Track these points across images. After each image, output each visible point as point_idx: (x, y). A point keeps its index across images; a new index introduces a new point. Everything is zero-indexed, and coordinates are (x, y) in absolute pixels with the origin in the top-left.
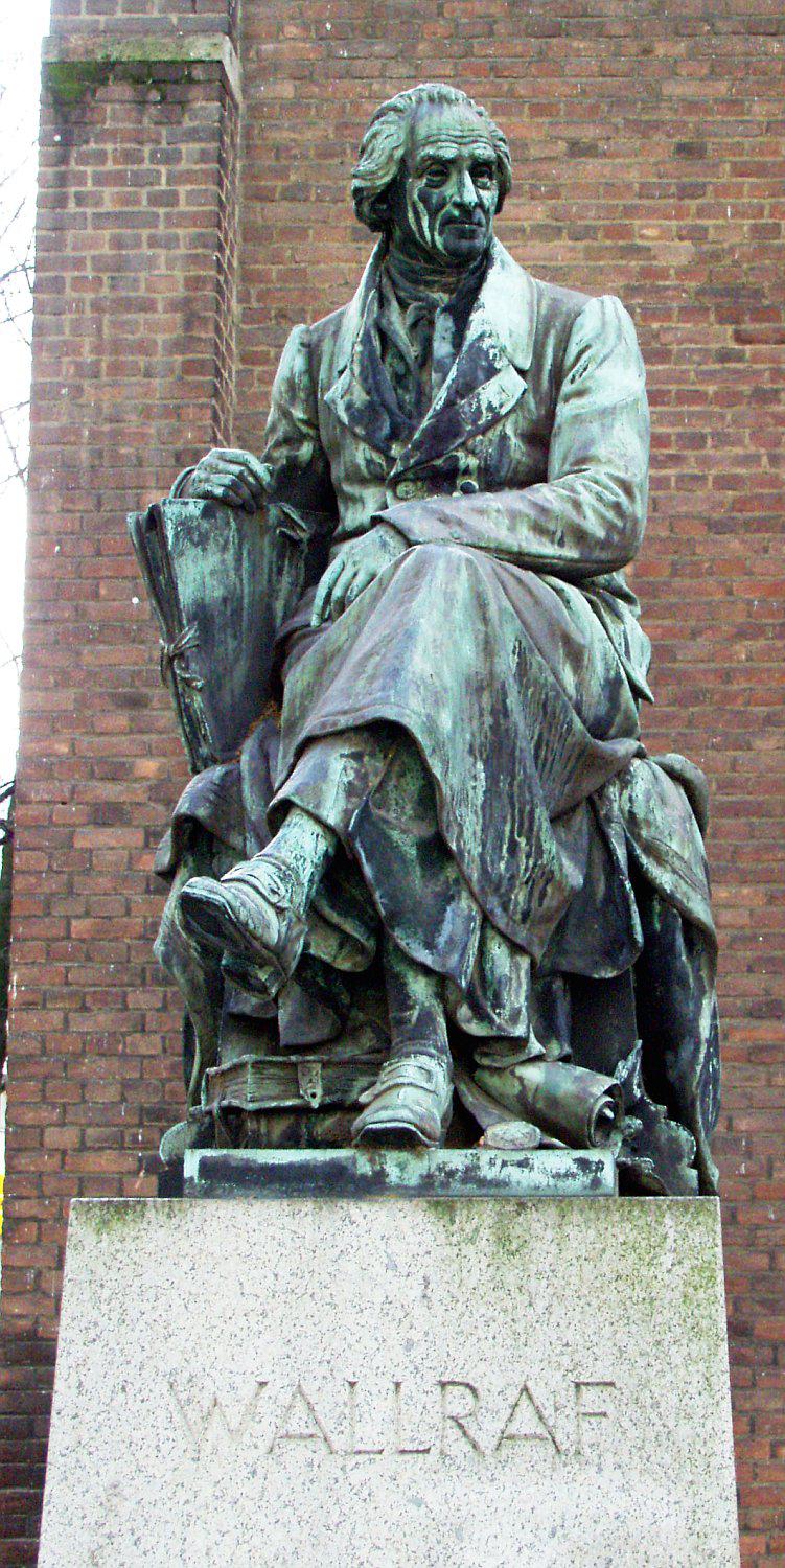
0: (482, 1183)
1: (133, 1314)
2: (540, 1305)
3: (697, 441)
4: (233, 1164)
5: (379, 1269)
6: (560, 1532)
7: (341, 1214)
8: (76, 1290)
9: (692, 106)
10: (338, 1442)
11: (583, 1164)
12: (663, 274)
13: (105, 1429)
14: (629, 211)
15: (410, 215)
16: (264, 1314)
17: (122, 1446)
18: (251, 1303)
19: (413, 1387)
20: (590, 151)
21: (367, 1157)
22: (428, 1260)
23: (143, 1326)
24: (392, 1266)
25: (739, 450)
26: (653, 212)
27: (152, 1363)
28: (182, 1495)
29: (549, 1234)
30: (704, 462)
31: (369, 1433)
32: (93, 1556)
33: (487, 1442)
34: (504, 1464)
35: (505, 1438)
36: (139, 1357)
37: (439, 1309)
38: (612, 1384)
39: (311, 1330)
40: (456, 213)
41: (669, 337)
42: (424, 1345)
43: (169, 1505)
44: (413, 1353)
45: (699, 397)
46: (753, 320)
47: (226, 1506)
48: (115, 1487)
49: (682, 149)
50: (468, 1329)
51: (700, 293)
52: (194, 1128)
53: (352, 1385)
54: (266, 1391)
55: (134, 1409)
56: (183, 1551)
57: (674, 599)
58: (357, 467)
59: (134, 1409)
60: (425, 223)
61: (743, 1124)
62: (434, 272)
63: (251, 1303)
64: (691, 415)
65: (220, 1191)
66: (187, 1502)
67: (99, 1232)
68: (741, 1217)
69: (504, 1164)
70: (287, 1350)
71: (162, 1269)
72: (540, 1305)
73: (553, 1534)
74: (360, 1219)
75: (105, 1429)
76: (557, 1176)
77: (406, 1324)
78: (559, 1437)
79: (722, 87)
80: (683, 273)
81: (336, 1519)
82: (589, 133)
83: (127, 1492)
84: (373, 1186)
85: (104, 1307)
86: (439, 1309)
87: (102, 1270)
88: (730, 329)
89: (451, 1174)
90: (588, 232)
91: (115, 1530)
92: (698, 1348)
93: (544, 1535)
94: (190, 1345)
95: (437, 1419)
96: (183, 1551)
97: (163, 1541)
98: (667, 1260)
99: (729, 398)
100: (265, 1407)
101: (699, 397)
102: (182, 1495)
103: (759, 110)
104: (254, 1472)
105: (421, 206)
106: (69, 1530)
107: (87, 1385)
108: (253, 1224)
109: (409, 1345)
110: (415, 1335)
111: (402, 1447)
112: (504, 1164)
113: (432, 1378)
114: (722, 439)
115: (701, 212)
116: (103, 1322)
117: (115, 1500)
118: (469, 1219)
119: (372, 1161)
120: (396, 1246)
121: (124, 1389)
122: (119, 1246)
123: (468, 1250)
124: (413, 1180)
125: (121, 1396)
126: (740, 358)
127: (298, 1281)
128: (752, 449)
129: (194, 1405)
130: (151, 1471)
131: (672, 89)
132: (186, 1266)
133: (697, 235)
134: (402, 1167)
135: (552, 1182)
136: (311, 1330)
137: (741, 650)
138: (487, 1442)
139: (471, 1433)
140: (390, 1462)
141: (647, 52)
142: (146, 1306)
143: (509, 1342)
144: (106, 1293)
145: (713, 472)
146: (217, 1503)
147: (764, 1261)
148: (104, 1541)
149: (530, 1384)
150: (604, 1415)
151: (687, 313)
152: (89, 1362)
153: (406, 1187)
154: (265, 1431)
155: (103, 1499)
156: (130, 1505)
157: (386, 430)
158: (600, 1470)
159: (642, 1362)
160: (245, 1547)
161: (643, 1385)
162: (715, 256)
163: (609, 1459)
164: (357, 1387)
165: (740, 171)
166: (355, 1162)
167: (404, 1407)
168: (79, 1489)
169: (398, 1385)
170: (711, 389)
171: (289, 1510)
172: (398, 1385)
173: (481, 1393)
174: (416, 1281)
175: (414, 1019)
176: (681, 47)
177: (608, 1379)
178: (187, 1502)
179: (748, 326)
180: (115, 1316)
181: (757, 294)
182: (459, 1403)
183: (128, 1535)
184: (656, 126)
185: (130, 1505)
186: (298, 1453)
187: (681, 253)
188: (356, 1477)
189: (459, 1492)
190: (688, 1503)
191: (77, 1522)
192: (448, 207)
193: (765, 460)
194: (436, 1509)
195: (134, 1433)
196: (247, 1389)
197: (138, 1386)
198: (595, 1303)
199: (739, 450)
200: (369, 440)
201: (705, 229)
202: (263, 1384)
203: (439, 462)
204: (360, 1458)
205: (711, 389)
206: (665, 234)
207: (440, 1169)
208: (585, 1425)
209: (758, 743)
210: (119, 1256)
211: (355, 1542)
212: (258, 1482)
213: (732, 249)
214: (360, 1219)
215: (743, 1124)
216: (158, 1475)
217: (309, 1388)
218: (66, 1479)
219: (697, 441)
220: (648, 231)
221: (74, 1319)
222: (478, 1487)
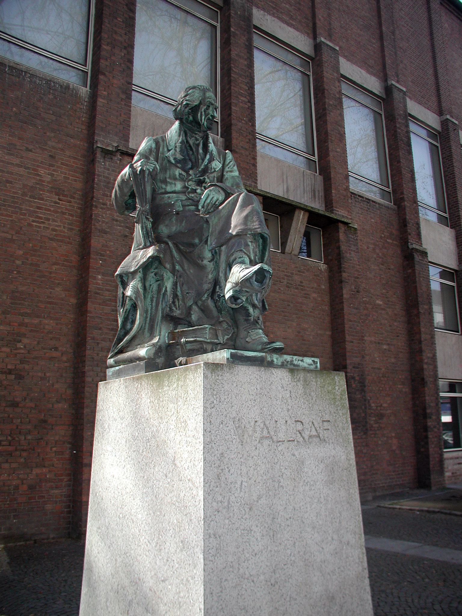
0: (294, 365)
1: (223, 399)
2: (314, 399)
3: (48, 220)
4: (239, 355)
5: (280, 388)
6: (323, 461)
7: (270, 371)
8: (207, 391)
9: (53, 147)
10: (275, 438)
11: (313, 361)
12: (43, 181)
13: (218, 436)
14: (38, 166)
15: (199, 115)
16: (255, 400)
17: (223, 441)
18: (252, 397)
19: (290, 422)
20: (31, 151)
21: (270, 356)
22: (290, 386)
23: (226, 403)
24: (283, 387)
25: (57, 224)
26: (43, 168)
27: (229, 415)
28: (240, 456)
29: (314, 380)
30: (49, 224)
31: (281, 436)
32: (218, 476)
33: (306, 438)
34: (310, 443)
35: (310, 436)
36: (225, 413)
37: (293, 400)
38: (329, 421)
39: (266, 405)
40: (211, 118)
41: (44, 196)
42: (292, 410)
43: (236, 459)
44: (289, 413)
45: (49, 210)
46: (63, 196)
47: (250, 458)
48: (222, 454)
49: (51, 156)
50: (300, 406)
51: (52, 188)
52: (154, 349)
53: (276, 421)
54: (257, 424)
55: (225, 429)
56: (241, 473)
57: (40, 254)
58: (176, 175)
59: (225, 429)
60: (203, 118)
61: (48, 374)
62: (198, 131)
63: (252, 397)
64: (47, 214)
65: (236, 363)
66: (241, 458)
67: (212, 373)
68: (46, 396)
69: (298, 360)
70: (261, 411)
71: (229, 386)
72: (314, 399)
73: (322, 462)
74: (275, 373)
75: (218, 436)
76: (309, 365)
77: (287, 404)
78: (321, 435)
79: (60, 146)
80: (48, 182)
81: (276, 461)
82: (31, 147)
83: (226, 455)
84: (271, 364)
85: (215, 397)
86: (293, 400)
87: (213, 385)
88: (57, 197)
89: (288, 362)
90: (28, 168)
91: (223, 468)
92: (344, 411)
93: (320, 462)
94: (238, 410)
95: (295, 432)
96: (241, 473)
97: (236, 470)
98: (337, 388)
99: (56, 212)
100: (258, 429)
101: (49, 210)
102: (240, 456)
103: (68, 153)
104: (256, 448)
105: (203, 113)
106: (211, 468)
107: (212, 422)
108: (250, 373)
109: (288, 410)
110: (290, 408)
111: (289, 439)
112: (298, 360)
113: (294, 419)
114: (54, 221)
115: (54, 170)
116: (215, 401)
117: (222, 458)
118: (298, 375)
119: (271, 357)
120: (283, 382)
121: (222, 423)
122: (217, 378)
123: (299, 384)
124: (280, 364)
125: (221, 426)
126: (59, 204)
127: (262, 391)
128: (60, 224)
129: (240, 428)
130: (231, 449)
131: (49, 143)
132: (235, 385)
133: (52, 175)
134: (277, 359)
135: (308, 366)
136: (266, 405)
137: (55, 267)
138: (306, 438)
139: (303, 435)
140: (286, 444)
141: (45, 133)
142: (226, 397)
143: (309, 409)
144: (215, 393)
145: (51, 227)
146: (248, 458)
147: (51, 406)
148: (220, 471)
149: (314, 421)
150: (328, 429)
151: (48, 191)
152: (212, 414)
153: (278, 365)
154: (258, 435)
155: (219, 458)
156: (227, 459)
157: (190, 166)
158: (329, 444)
159: (334, 415)
160: (256, 471)
161: (335, 421)
162: (56, 181)
163: (331, 441)
164: (278, 423)
165: (62, 164)
166: (266, 357)
167: (289, 428)
168: (213, 455)
169: (286, 421)
170: (52, 209)
171: (265, 459)
172: (286, 421)
173: (304, 424)
174: (288, 392)
175: (252, 320)
176: (53, 135)
177: (329, 420)
178: (241, 458)
179: (61, 197)
180: (218, 400)
181: (64, 191)
182: (299, 427)
183: (227, 469)
184: (46, 150)
185: (227, 459)
186: (266, 442)
187: (48, 178)
188: (280, 448)
189: (302, 451)
190: (346, 451)
191: (213, 466)
192: (209, 116)
193: (62, 227)
194: (297, 456)
195: (226, 437)
196: (252, 424)
197: (225, 422)
198: (324, 399)
199: (57, 224)
200: (183, 169)
201: (54, 174)
202: (256, 422)
203: (201, 178)
204: (280, 443)
205: (52, 209)
206: (45, 173)
207: (285, 361)
208: (325, 432)
209: (56, 289)
210: (218, 381)
211: (281, 468)
212: (257, 451)
213: (59, 180)
214: (275, 373)
215: (48, 374)
216: (233, 450)
217: (267, 423)
218: (209, 452)
219: (48, 220)
220: (42, 172)
221: (207, 400)
222: (305, 450)
